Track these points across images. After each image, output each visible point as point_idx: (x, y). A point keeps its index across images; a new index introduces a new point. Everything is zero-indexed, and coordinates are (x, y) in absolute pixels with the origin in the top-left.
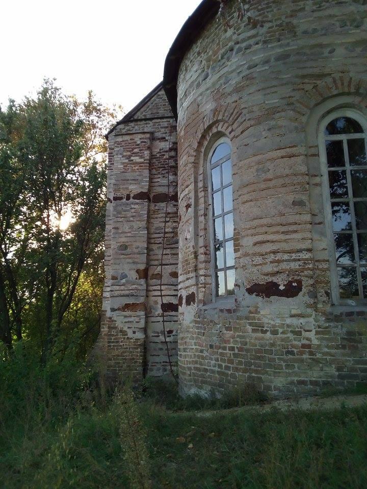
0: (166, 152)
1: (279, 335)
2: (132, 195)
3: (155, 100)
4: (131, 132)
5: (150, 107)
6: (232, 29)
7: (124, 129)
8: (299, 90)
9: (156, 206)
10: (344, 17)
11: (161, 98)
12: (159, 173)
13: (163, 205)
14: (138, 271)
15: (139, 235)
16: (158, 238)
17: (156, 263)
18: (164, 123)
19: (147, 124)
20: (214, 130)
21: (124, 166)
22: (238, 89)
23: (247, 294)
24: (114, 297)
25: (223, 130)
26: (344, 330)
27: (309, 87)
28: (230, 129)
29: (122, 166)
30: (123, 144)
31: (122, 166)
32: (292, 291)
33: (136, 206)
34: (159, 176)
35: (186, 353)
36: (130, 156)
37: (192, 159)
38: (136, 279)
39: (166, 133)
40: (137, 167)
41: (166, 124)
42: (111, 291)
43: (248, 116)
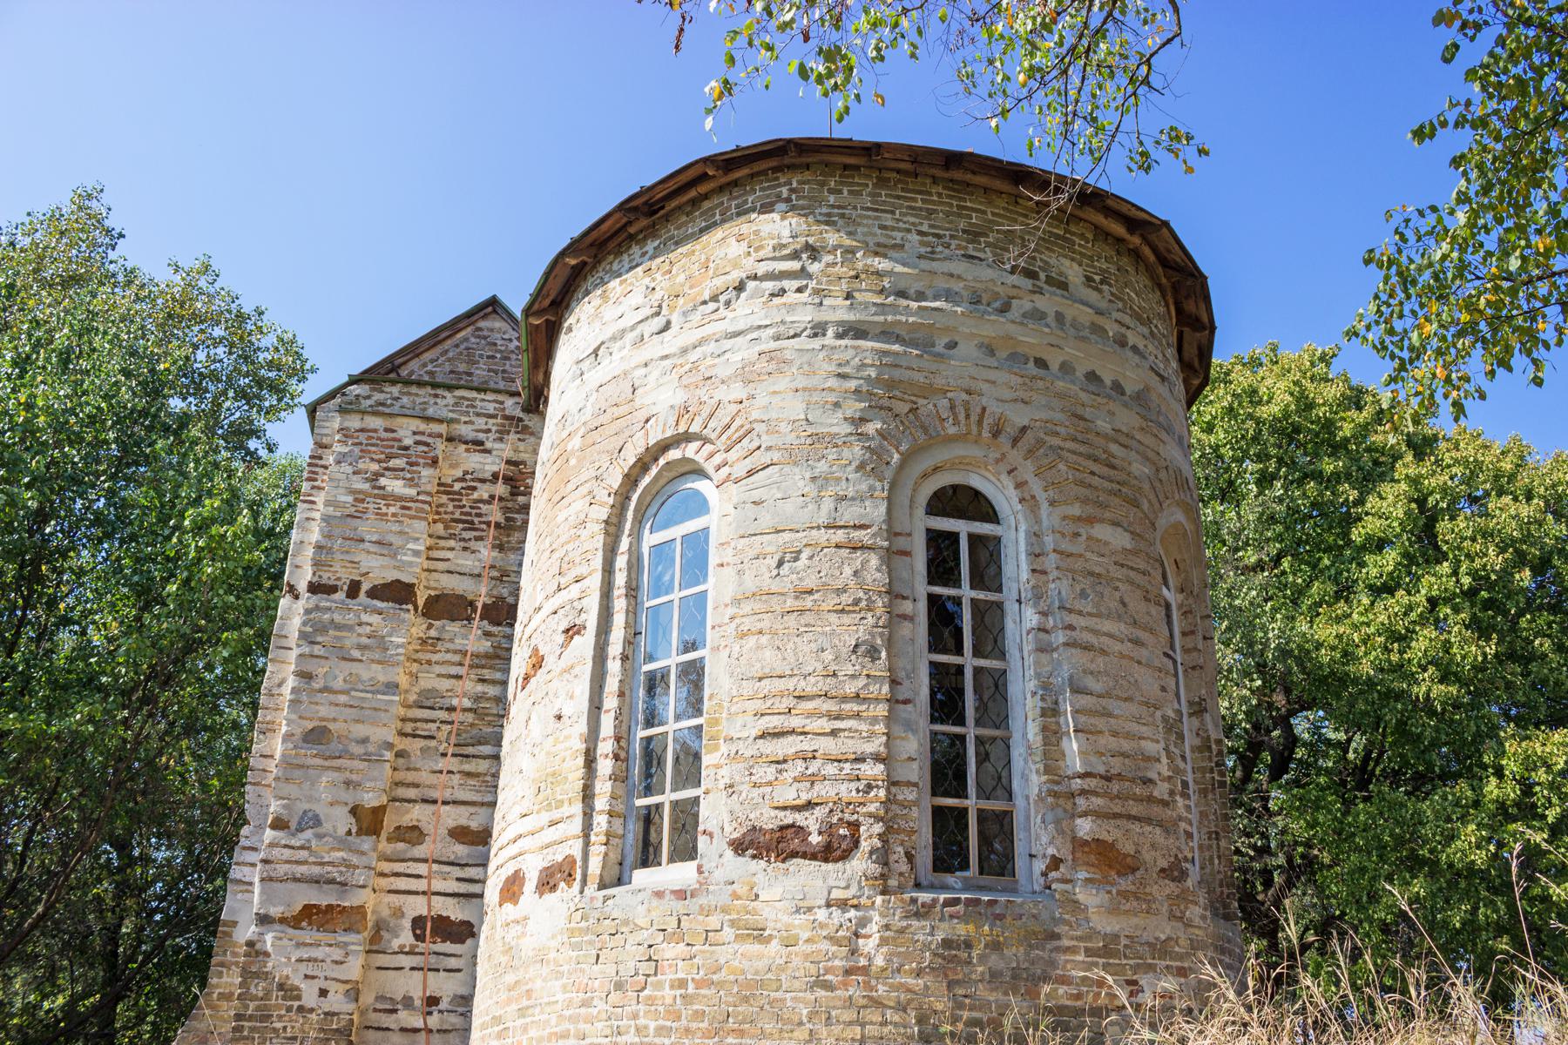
0: (483, 481)
1: (802, 947)
2: (365, 587)
3: (466, 339)
4: (387, 410)
5: (451, 354)
6: (744, 244)
7: (369, 397)
8: (881, 408)
9: (430, 627)
10: (978, 285)
11: (485, 338)
12: (452, 536)
13: (453, 628)
14: (354, 811)
15: (374, 705)
16: (427, 721)
17: (412, 793)
18: (488, 403)
19: (436, 396)
20: (674, 454)
21: (356, 500)
22: (746, 376)
23: (729, 853)
24: (271, 879)
25: (699, 458)
26: (939, 937)
27: (902, 408)
28: (717, 459)
29: (350, 499)
30: (362, 437)
31: (350, 499)
33: (375, 619)
34: (452, 543)
35: (528, 1020)
36: (377, 475)
37: (603, 513)
38: (349, 833)
39: (489, 431)
40: (392, 510)
41: (491, 408)
42: (265, 861)
43: (766, 441)
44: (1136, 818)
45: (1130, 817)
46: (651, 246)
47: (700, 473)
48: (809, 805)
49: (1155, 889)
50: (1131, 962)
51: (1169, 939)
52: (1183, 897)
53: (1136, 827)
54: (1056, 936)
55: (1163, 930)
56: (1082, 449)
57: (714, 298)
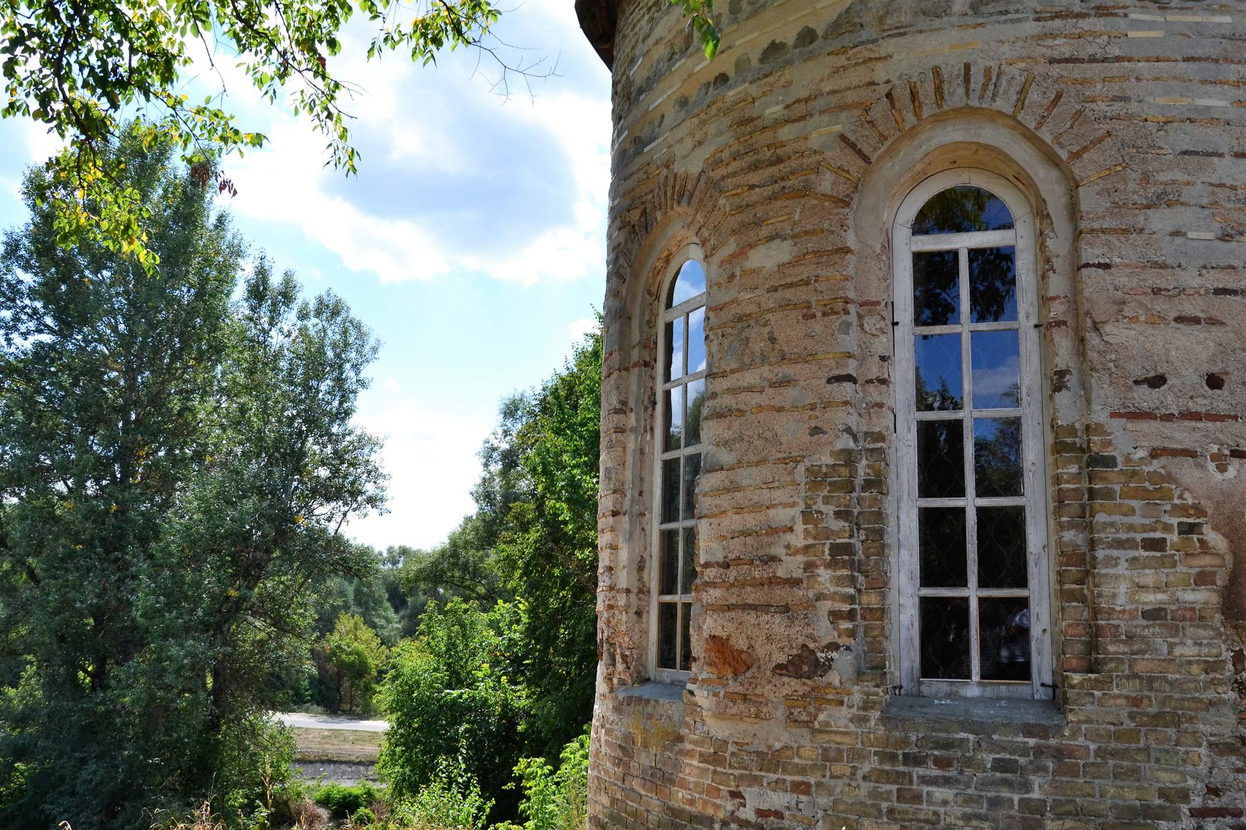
44: (754, 607)
45: (746, 607)
49: (767, 690)
50: (736, 772)
51: (786, 748)
52: (818, 698)
53: (751, 618)
54: (680, 739)
55: (778, 736)
56: (749, 159)
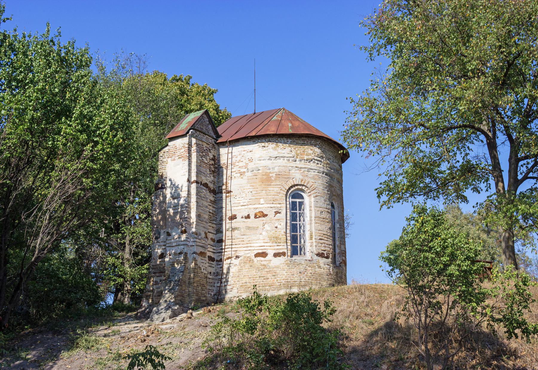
22: (313, 178)
32: (327, 258)
46: (290, 141)
47: (303, 191)
48: (325, 251)
57: (307, 160)
